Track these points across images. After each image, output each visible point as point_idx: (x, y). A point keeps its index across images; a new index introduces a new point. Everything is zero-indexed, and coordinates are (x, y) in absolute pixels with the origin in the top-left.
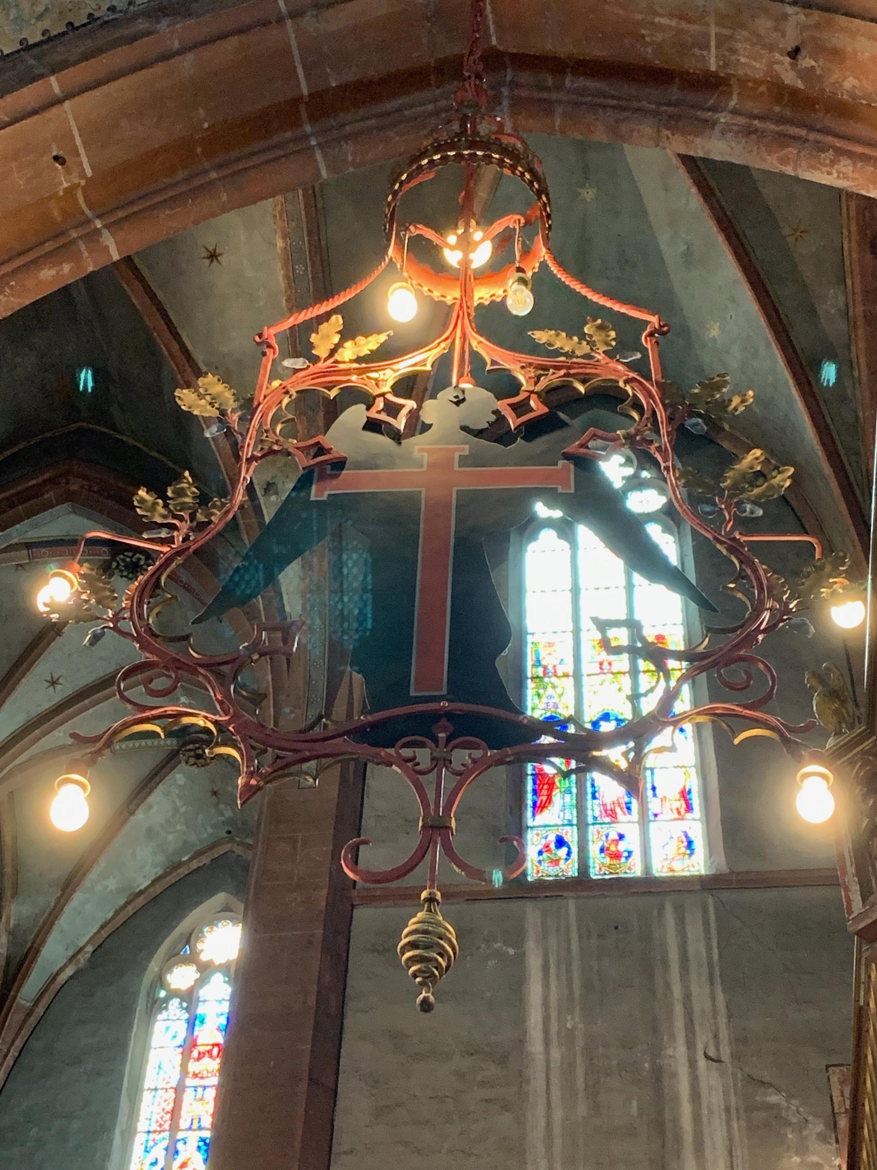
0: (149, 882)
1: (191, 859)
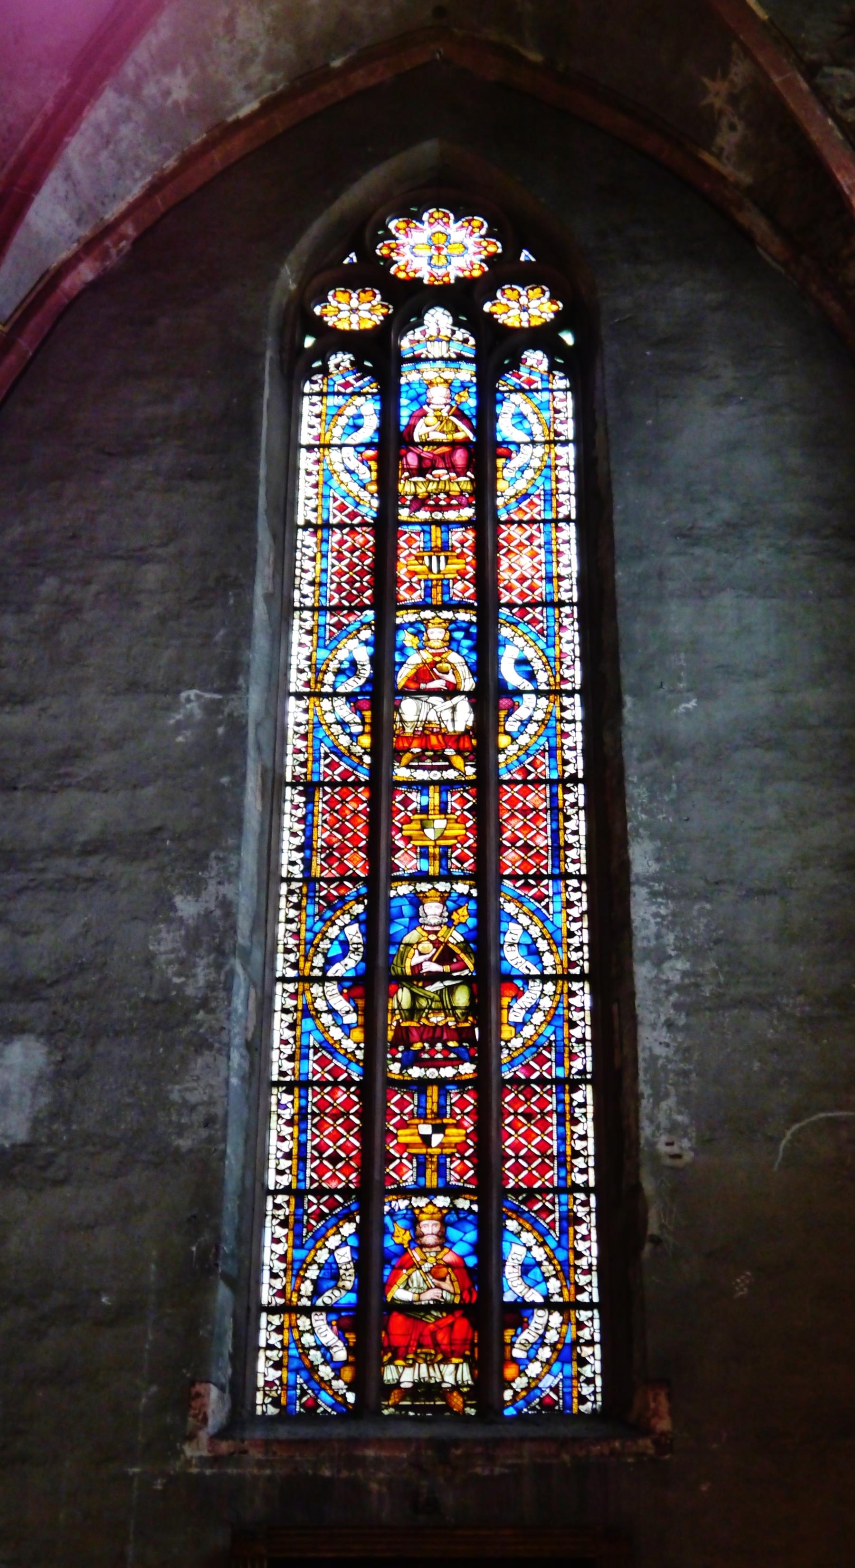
0: (255, 105)
1: (349, 67)
